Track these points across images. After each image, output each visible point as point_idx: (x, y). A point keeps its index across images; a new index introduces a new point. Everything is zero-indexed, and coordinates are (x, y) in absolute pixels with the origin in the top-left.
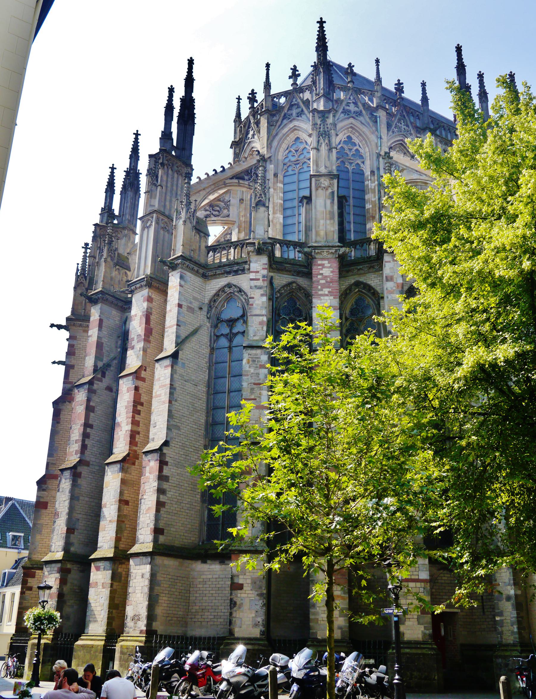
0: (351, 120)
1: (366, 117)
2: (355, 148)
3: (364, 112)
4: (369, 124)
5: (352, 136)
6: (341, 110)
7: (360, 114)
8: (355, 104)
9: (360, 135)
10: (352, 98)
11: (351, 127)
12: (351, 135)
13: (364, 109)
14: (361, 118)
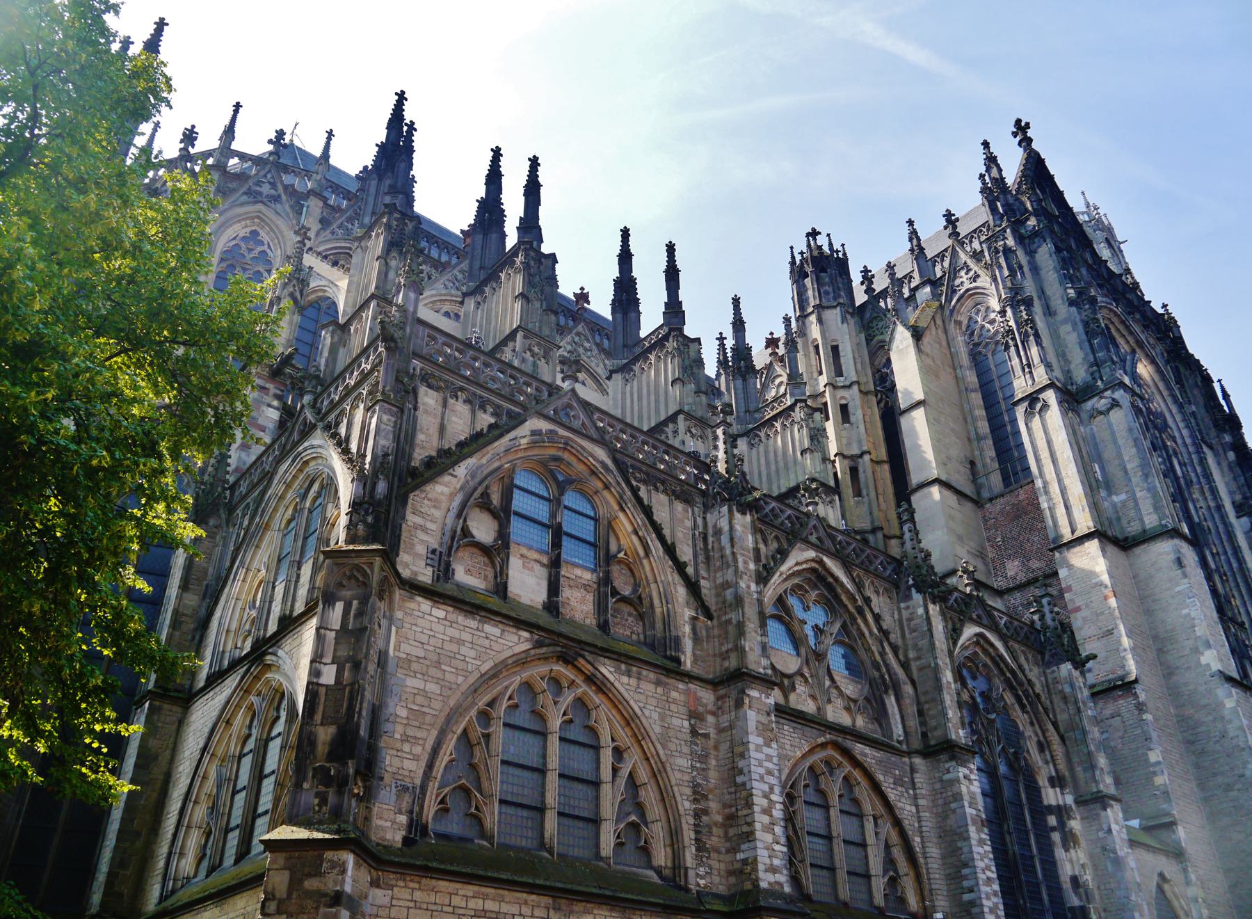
0: (260, 207)
1: (286, 206)
2: (260, 249)
3: (284, 197)
4: (288, 215)
5: (260, 231)
6: (244, 189)
7: (277, 199)
8: (273, 185)
9: (272, 229)
10: (269, 176)
11: (258, 217)
12: (258, 229)
13: (285, 192)
14: (278, 206)
